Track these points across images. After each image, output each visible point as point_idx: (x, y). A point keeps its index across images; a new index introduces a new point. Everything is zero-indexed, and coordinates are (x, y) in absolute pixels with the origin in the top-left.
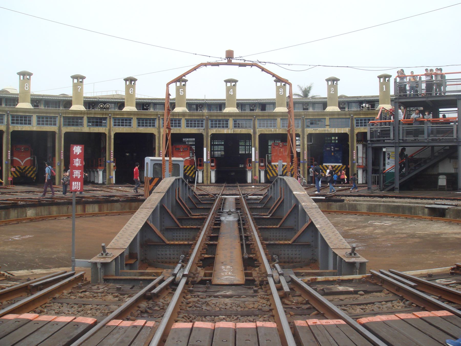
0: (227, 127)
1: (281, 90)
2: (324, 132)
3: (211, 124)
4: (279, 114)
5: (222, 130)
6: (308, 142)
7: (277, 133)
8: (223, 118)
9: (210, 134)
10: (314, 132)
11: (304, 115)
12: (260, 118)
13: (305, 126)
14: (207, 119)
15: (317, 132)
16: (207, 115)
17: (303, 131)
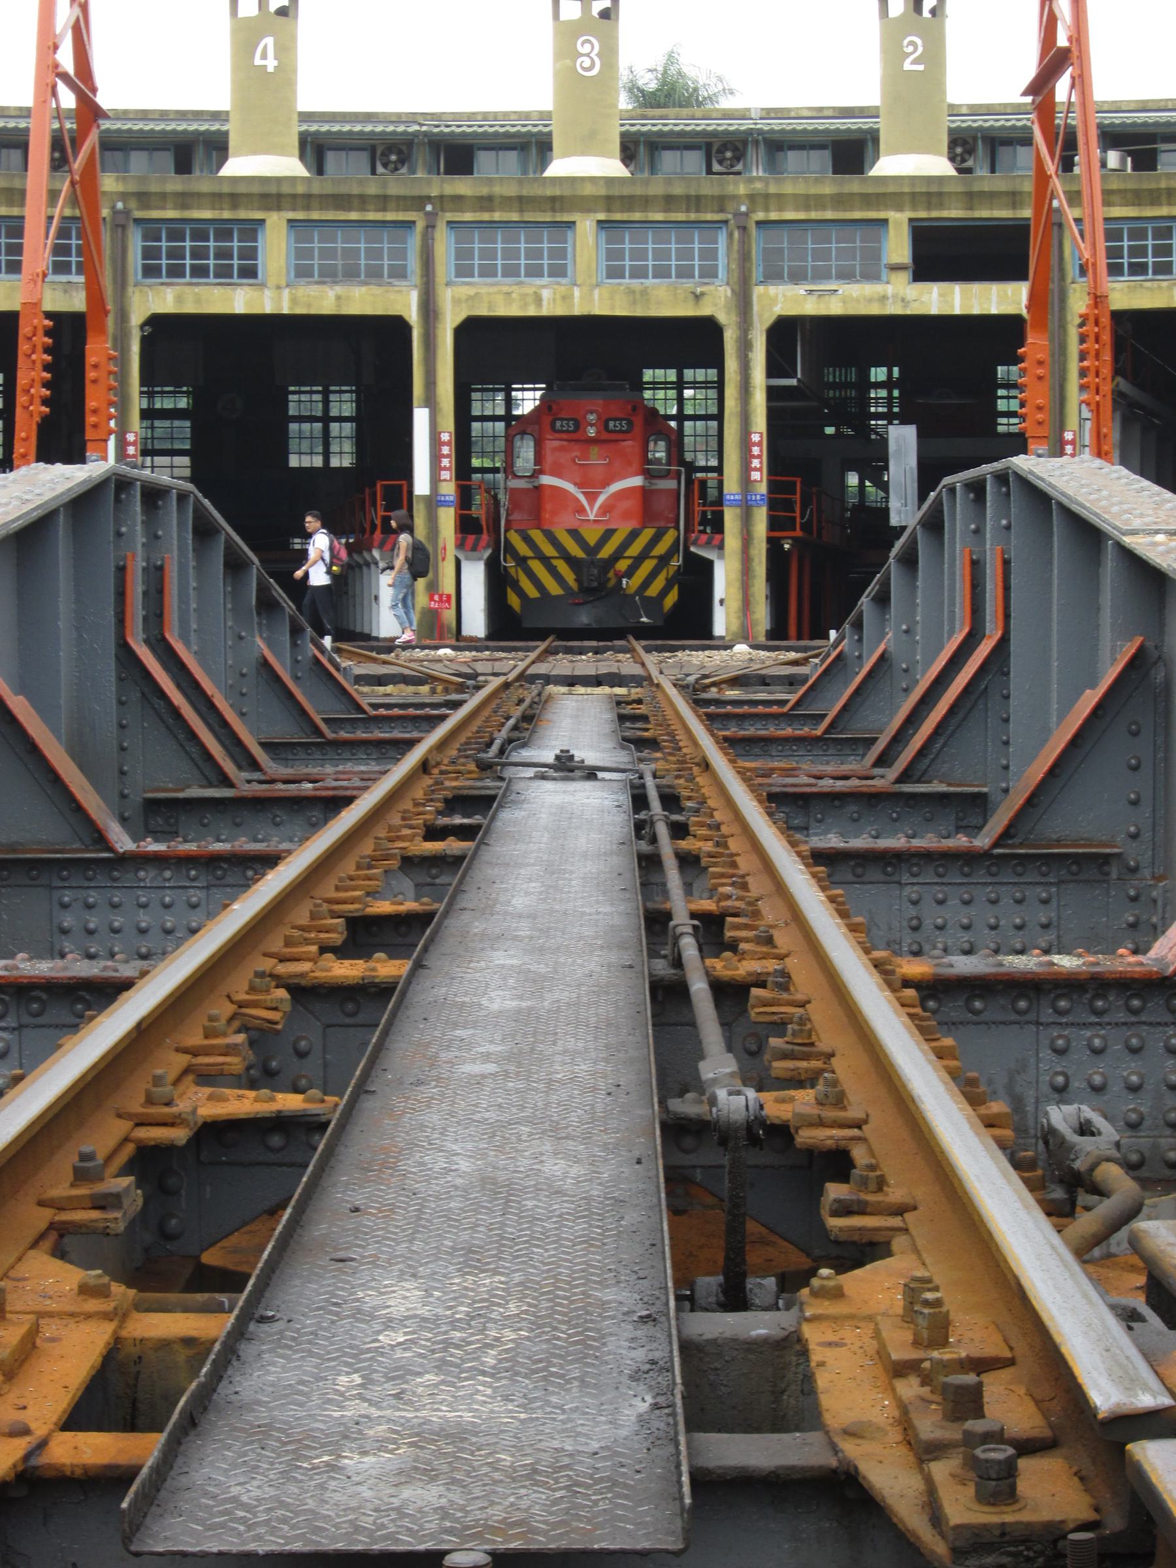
0: (249, 272)
1: (588, 47)
2: (875, 310)
3: (148, 253)
4: (588, 190)
5: (218, 291)
6: (772, 370)
7: (577, 311)
8: (226, 215)
9: (136, 318)
10: (811, 308)
11: (752, 198)
12: (468, 216)
13: (757, 273)
14: (121, 223)
15: (834, 308)
16: (124, 196)
17: (743, 303)
